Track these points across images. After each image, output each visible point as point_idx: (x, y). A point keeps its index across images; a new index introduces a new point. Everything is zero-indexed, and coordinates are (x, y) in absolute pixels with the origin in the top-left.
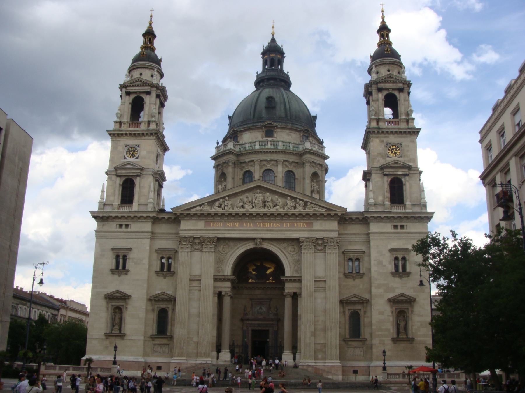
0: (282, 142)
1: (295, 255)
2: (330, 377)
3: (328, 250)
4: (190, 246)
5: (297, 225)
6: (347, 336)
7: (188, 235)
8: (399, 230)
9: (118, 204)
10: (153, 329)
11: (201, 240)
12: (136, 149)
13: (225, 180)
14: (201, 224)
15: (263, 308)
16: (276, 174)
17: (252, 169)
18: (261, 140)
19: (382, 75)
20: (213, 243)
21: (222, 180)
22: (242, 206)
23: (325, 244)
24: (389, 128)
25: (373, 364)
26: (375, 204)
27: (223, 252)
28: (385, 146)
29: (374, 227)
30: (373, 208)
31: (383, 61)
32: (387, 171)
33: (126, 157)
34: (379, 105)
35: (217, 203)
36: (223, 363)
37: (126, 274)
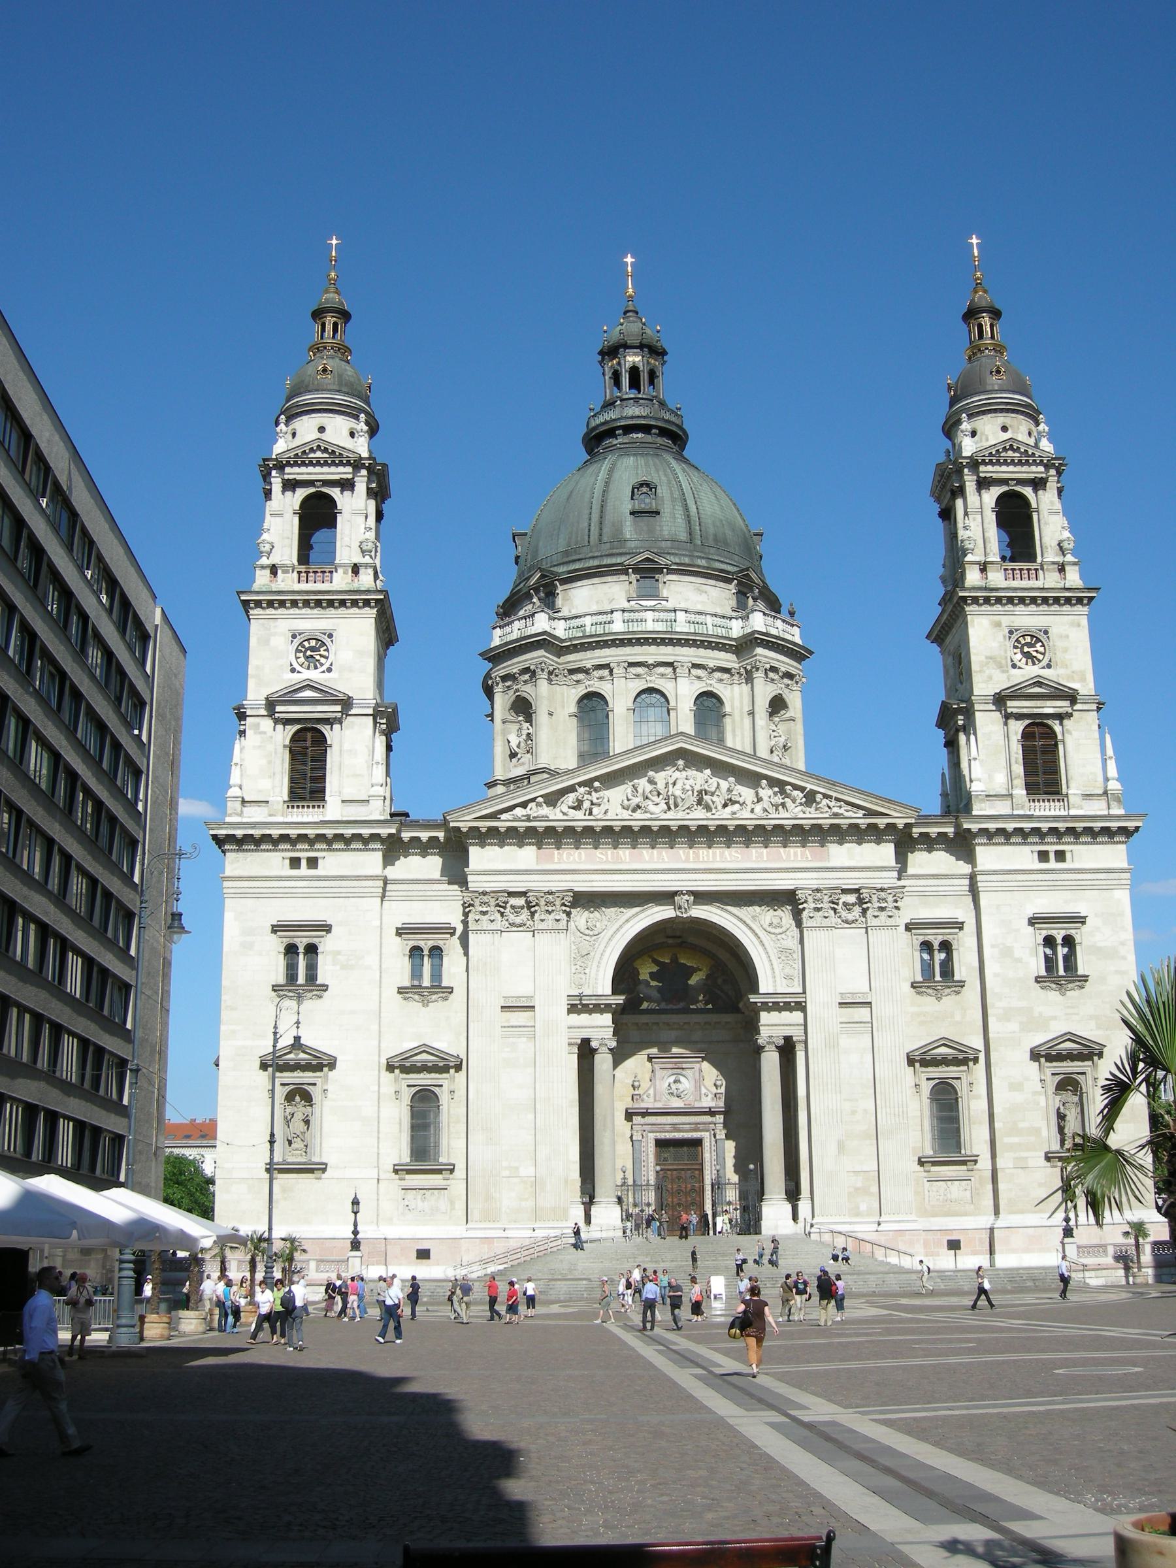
0: (686, 611)
1: (783, 936)
2: (893, 1259)
3: (872, 922)
4: (498, 916)
5: (789, 855)
6: (929, 1152)
7: (492, 884)
8: (1053, 864)
9: (285, 802)
10: (399, 1149)
11: (531, 899)
12: (324, 644)
13: (529, 719)
14: (527, 856)
15: (682, 1079)
16: (672, 704)
17: (604, 688)
18: (626, 605)
19: (987, 440)
20: (564, 908)
21: (521, 718)
22: (639, 807)
23: (865, 906)
24: (1015, 589)
25: (999, 1224)
26: (987, 796)
27: (587, 932)
28: (1005, 636)
29: (988, 856)
30: (983, 805)
31: (990, 404)
32: (1013, 706)
33: (298, 668)
34: (986, 526)
35: (571, 798)
36: (604, 1235)
37: (320, 997)
